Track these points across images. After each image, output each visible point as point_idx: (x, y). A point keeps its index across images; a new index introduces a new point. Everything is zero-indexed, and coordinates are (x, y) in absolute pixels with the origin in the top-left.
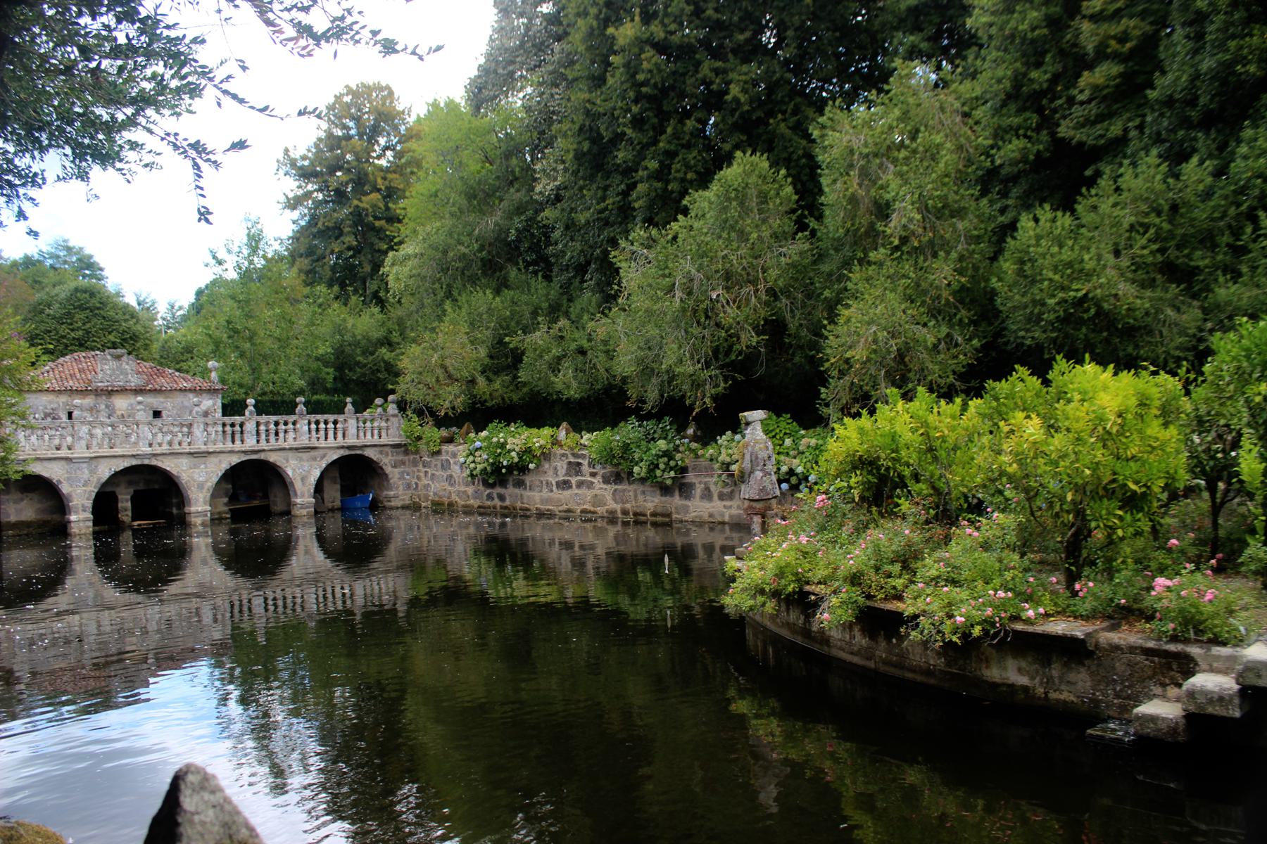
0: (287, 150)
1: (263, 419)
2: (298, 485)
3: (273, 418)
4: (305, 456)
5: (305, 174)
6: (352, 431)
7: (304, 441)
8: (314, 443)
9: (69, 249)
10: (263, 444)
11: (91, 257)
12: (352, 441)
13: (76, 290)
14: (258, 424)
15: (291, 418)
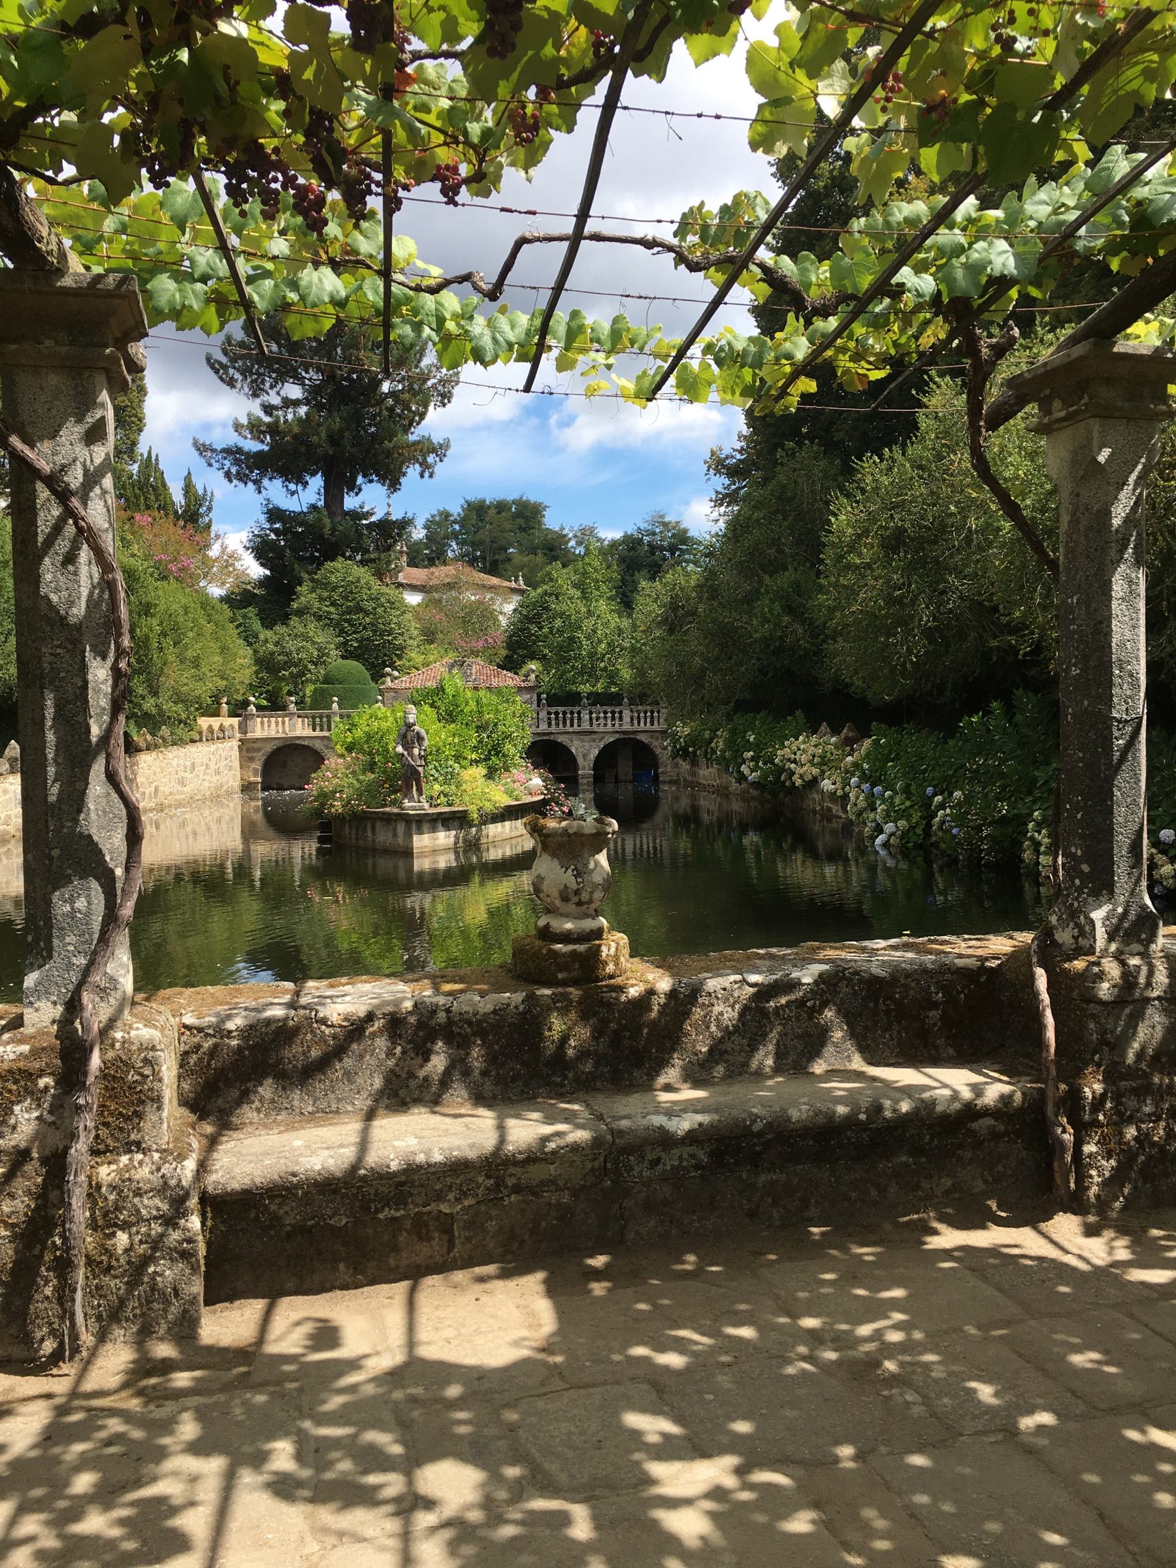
0: (713, 453)
1: (553, 709)
2: (580, 760)
3: (560, 709)
4: (586, 738)
5: (734, 472)
6: (626, 719)
7: (586, 726)
8: (595, 728)
9: (665, 524)
10: (553, 729)
11: (686, 531)
12: (627, 727)
13: (546, 593)
14: (549, 713)
15: (577, 709)
